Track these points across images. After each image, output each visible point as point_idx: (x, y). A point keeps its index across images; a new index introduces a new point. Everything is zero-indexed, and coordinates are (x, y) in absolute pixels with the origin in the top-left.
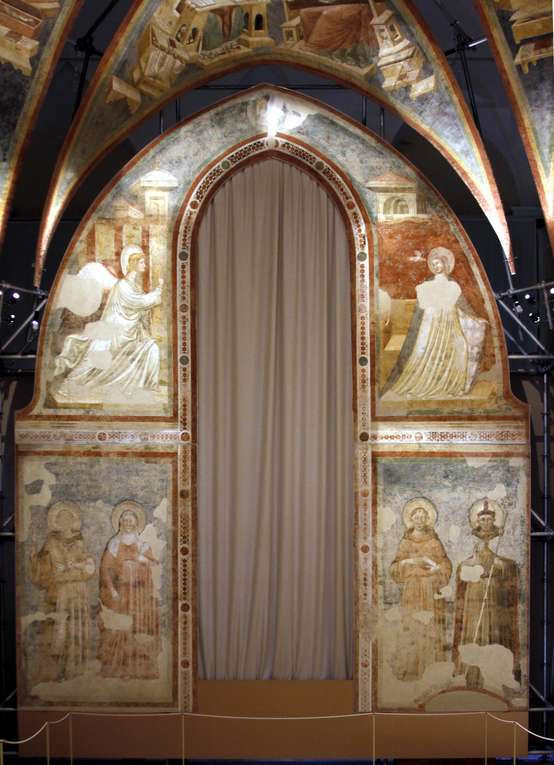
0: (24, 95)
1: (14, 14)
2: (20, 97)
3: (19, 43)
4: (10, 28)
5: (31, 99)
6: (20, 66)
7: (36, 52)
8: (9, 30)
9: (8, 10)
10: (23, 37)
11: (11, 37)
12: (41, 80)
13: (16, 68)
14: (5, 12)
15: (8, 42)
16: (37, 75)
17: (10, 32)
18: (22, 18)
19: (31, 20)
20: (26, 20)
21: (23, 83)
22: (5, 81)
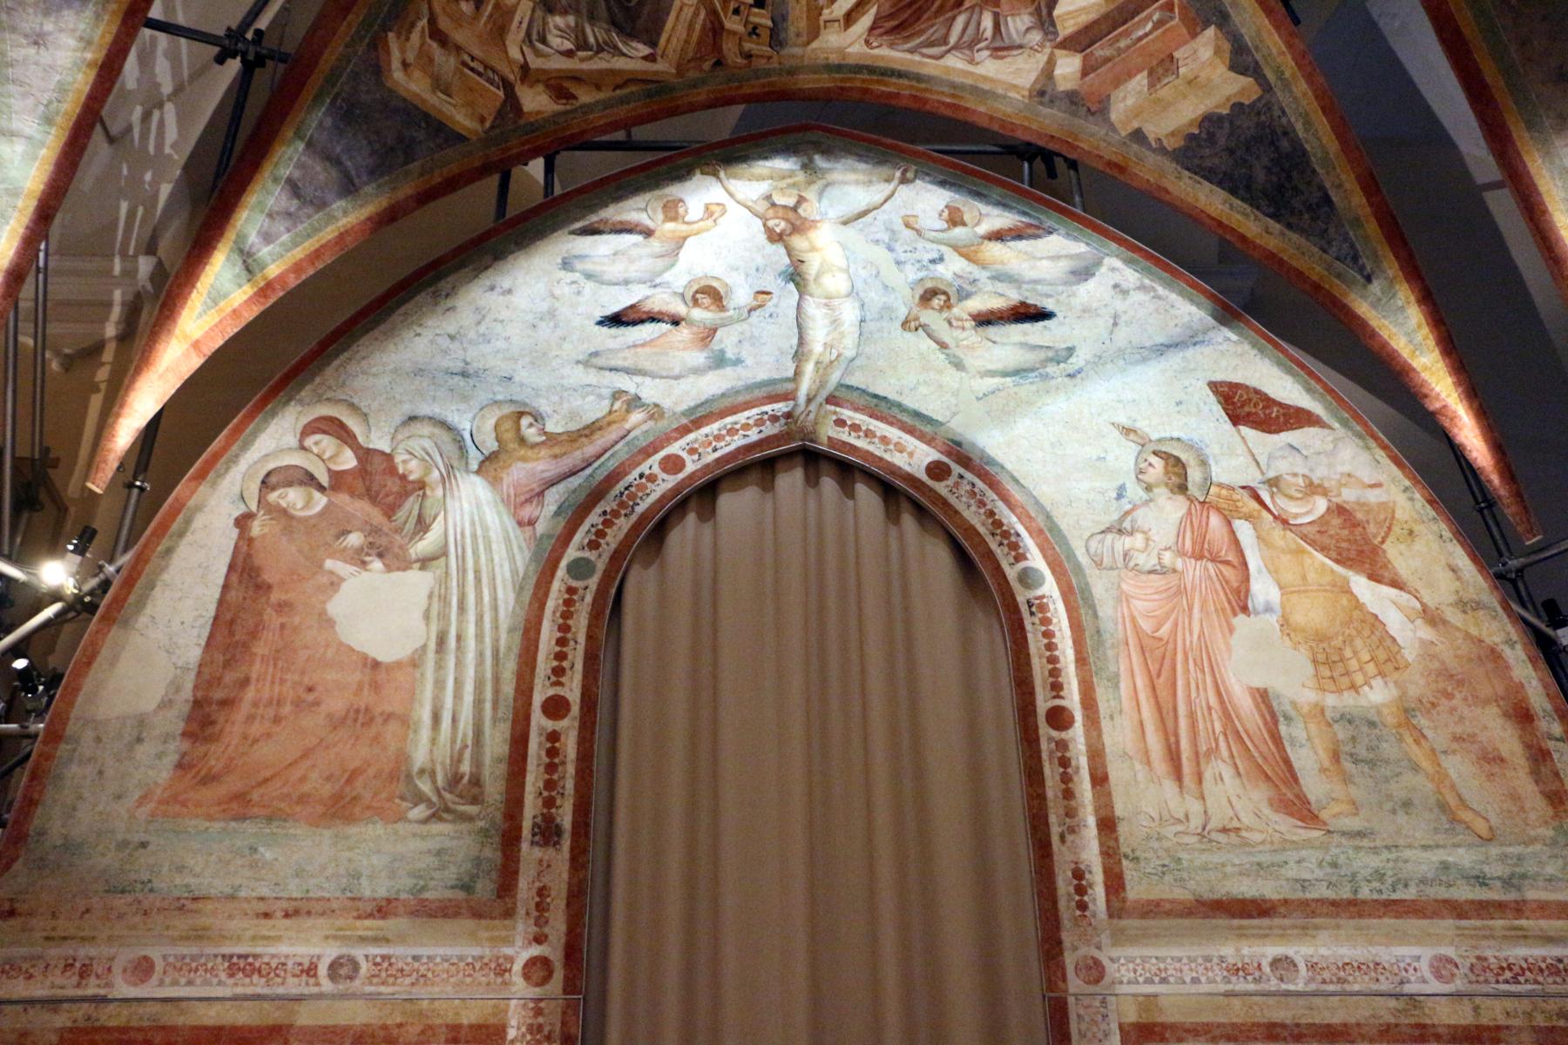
0: (1288, 132)
1: (1122, 44)
2: (1285, 144)
3: (1182, 70)
4: (1143, 69)
5: (1308, 124)
6: (1228, 99)
7: (1227, 46)
8: (1145, 73)
9: (1108, 52)
10: (1177, 55)
11: (1159, 80)
12: (1287, 74)
13: (1225, 111)
14: (1107, 60)
15: (1164, 92)
16: (1271, 76)
17: (1150, 74)
18: (1141, 33)
19: (1156, 17)
20: (1149, 26)
21: (1263, 118)
22: (1231, 152)
